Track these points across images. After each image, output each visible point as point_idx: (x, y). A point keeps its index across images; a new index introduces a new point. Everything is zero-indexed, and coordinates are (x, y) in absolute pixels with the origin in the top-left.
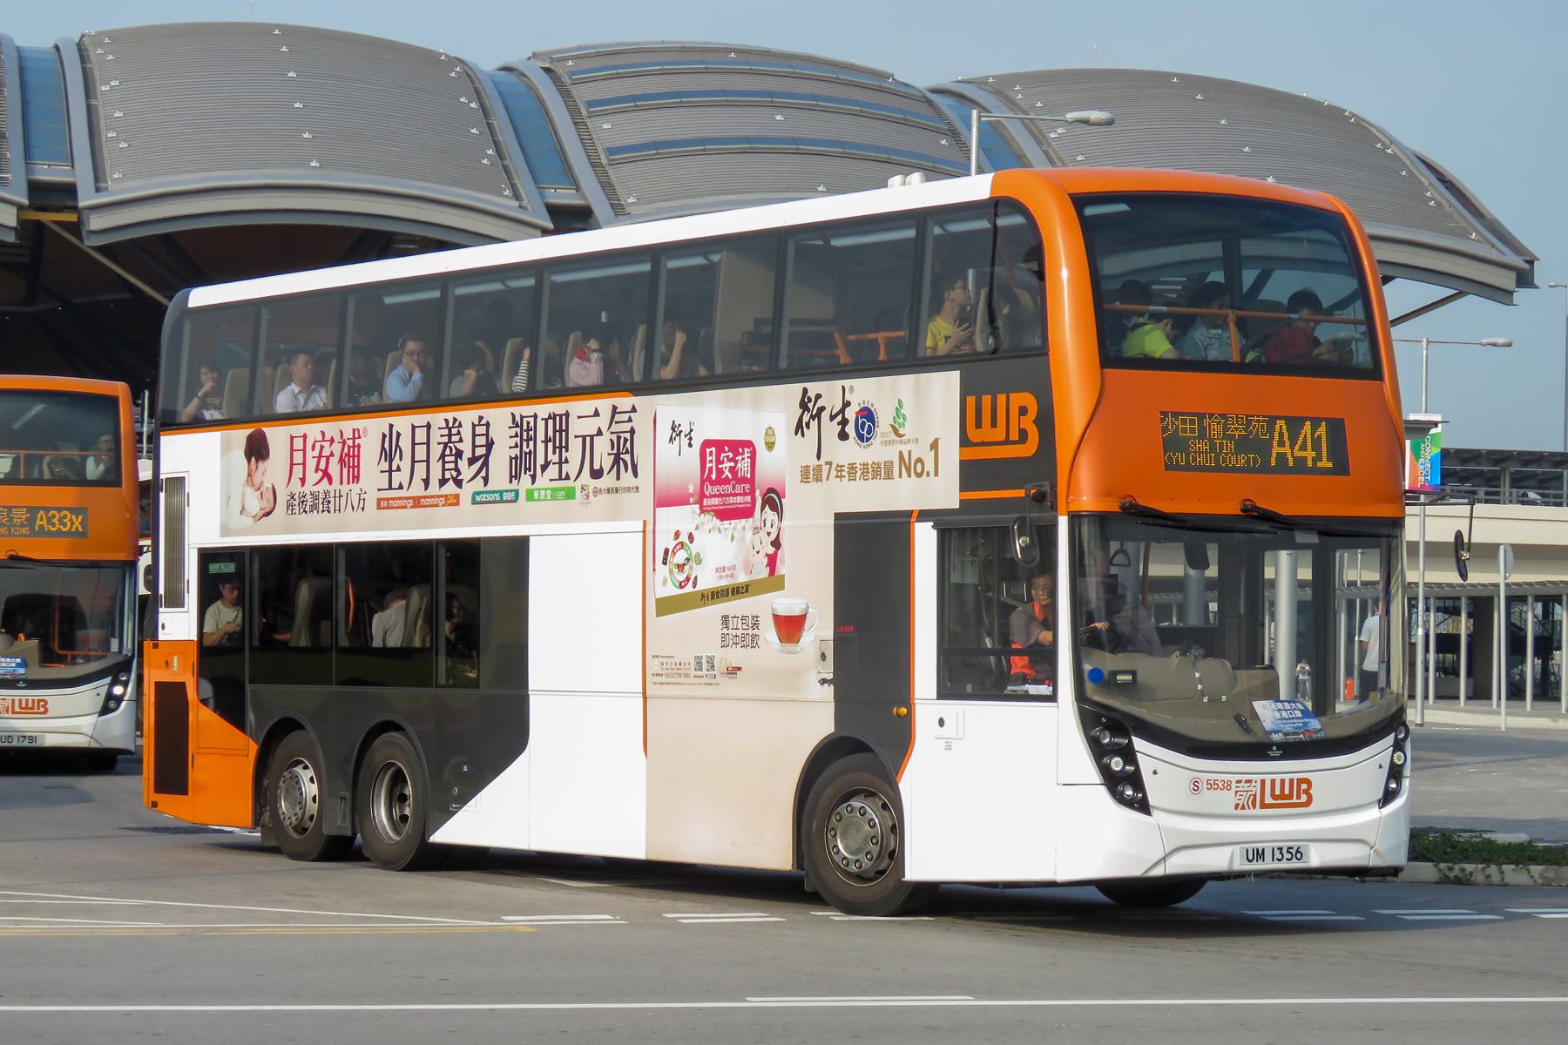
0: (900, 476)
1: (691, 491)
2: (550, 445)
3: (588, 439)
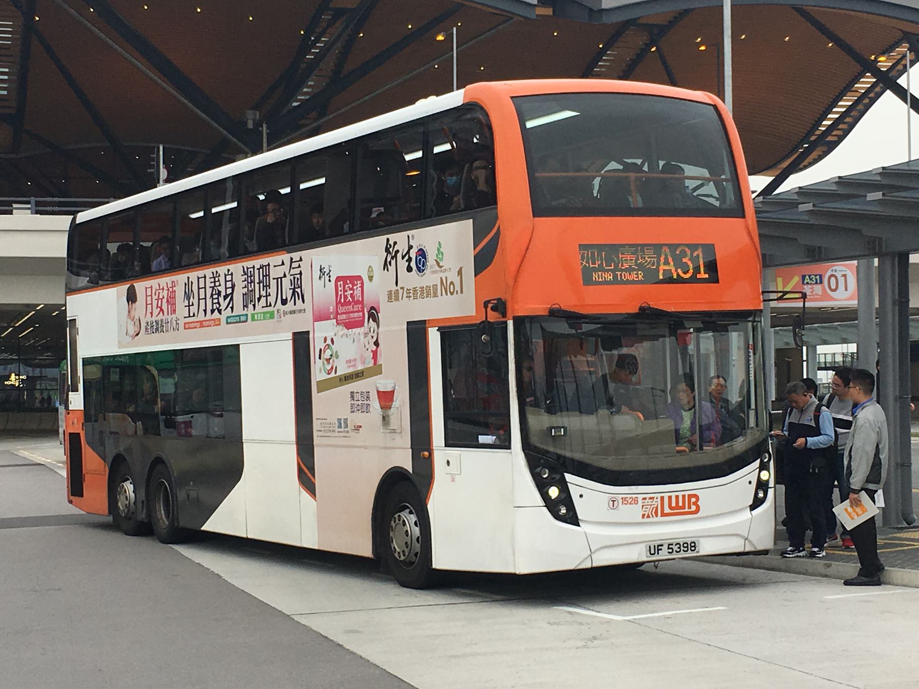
0: (442, 295)
1: (331, 311)
2: (261, 284)
3: (279, 280)
